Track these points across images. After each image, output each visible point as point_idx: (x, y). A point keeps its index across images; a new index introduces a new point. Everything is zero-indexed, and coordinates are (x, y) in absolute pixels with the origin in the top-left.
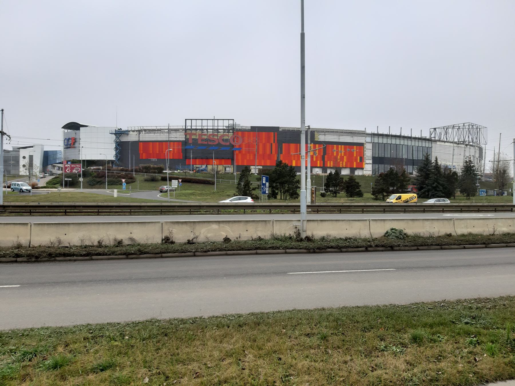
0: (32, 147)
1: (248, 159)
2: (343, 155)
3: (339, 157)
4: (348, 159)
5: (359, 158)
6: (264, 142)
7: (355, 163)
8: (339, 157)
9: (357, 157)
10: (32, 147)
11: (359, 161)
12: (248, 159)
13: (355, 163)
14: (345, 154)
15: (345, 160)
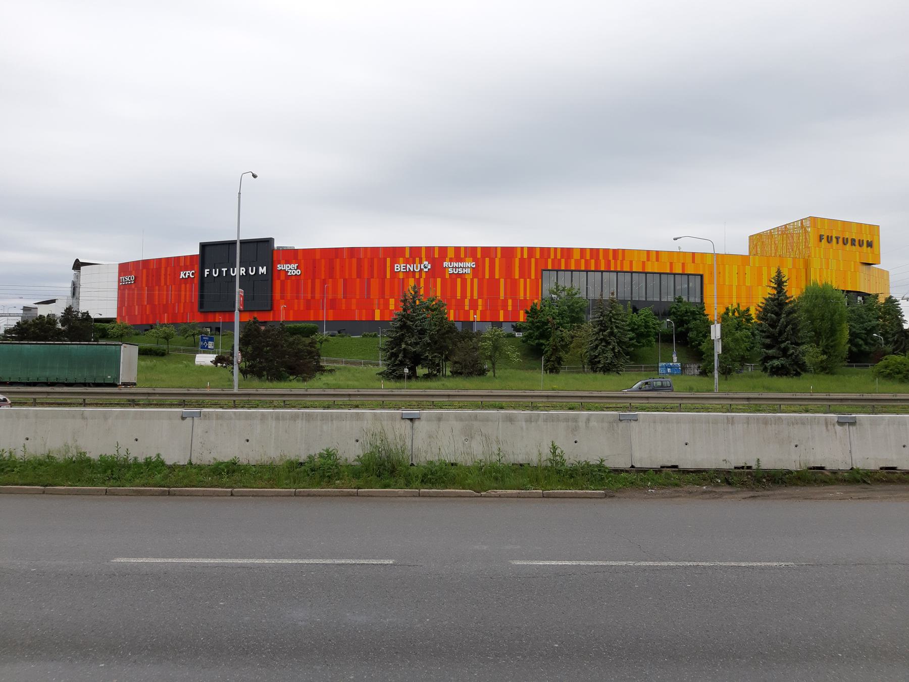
0: (53, 301)
1: (296, 308)
2: (475, 297)
3: (467, 302)
4: (485, 304)
5: (510, 302)
6: (323, 277)
7: (502, 312)
8: (467, 302)
9: (505, 302)
10: (53, 301)
11: (510, 308)
12: (296, 308)
13: (502, 312)
14: (480, 295)
15: (480, 308)
